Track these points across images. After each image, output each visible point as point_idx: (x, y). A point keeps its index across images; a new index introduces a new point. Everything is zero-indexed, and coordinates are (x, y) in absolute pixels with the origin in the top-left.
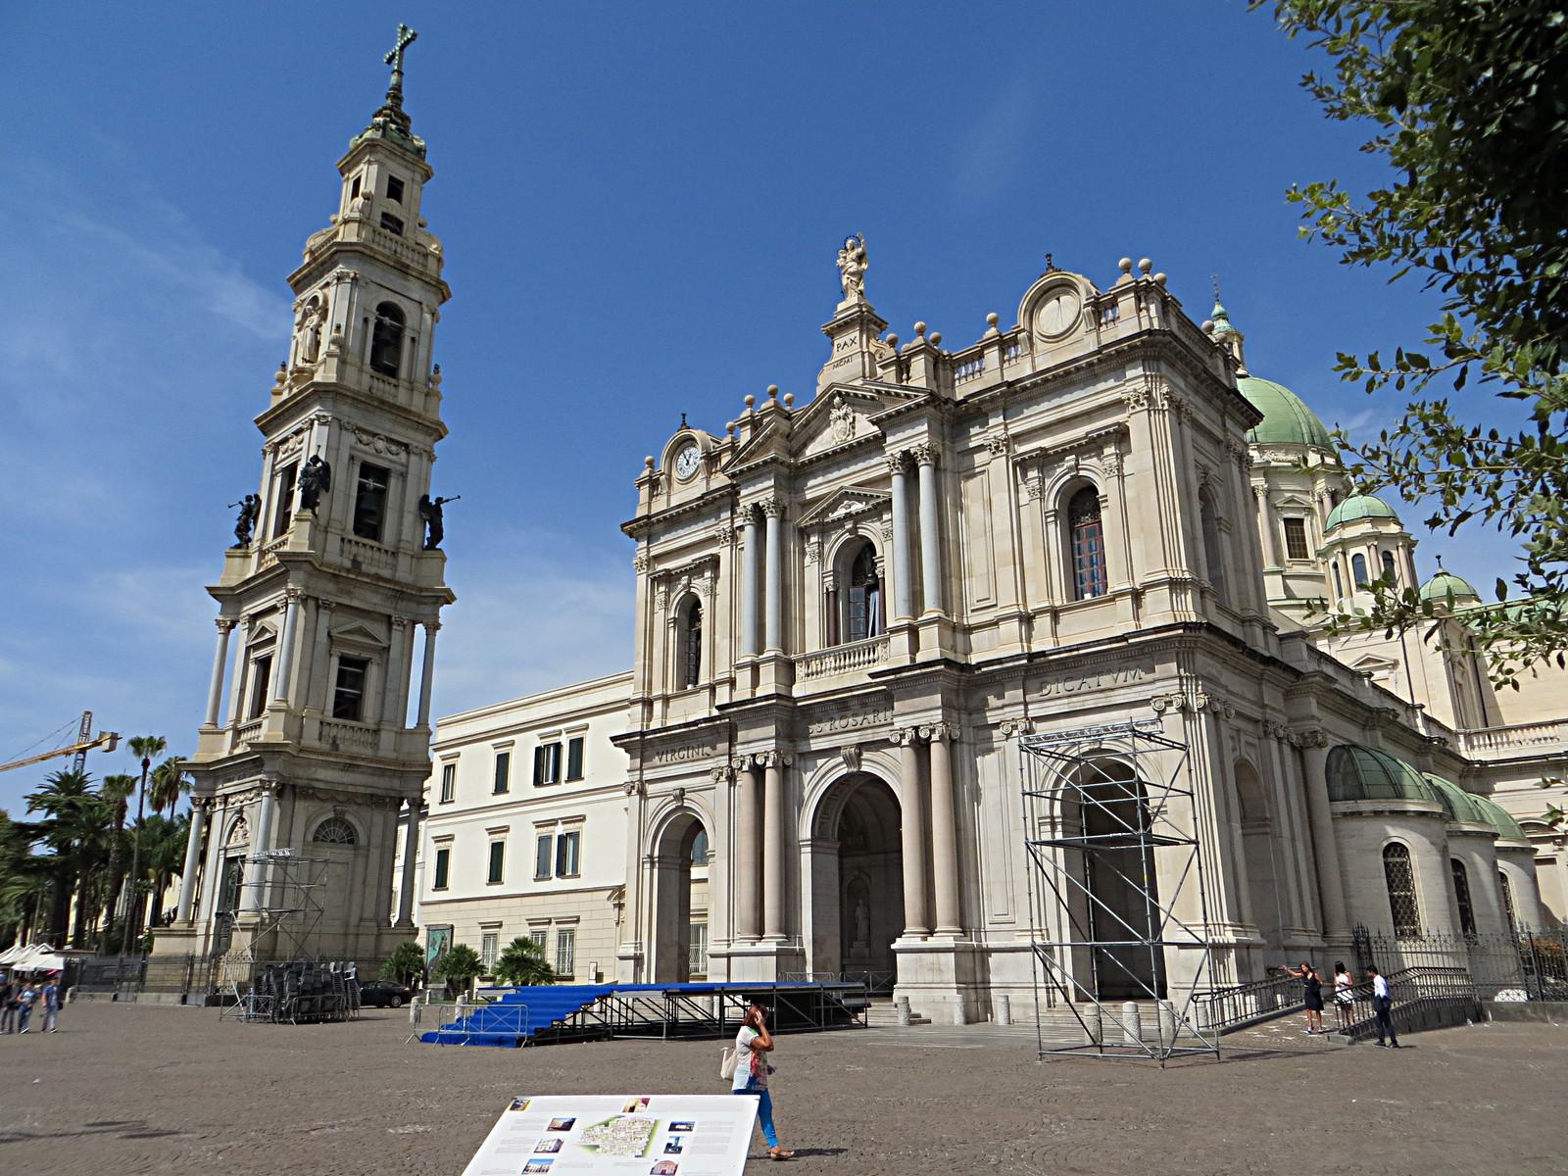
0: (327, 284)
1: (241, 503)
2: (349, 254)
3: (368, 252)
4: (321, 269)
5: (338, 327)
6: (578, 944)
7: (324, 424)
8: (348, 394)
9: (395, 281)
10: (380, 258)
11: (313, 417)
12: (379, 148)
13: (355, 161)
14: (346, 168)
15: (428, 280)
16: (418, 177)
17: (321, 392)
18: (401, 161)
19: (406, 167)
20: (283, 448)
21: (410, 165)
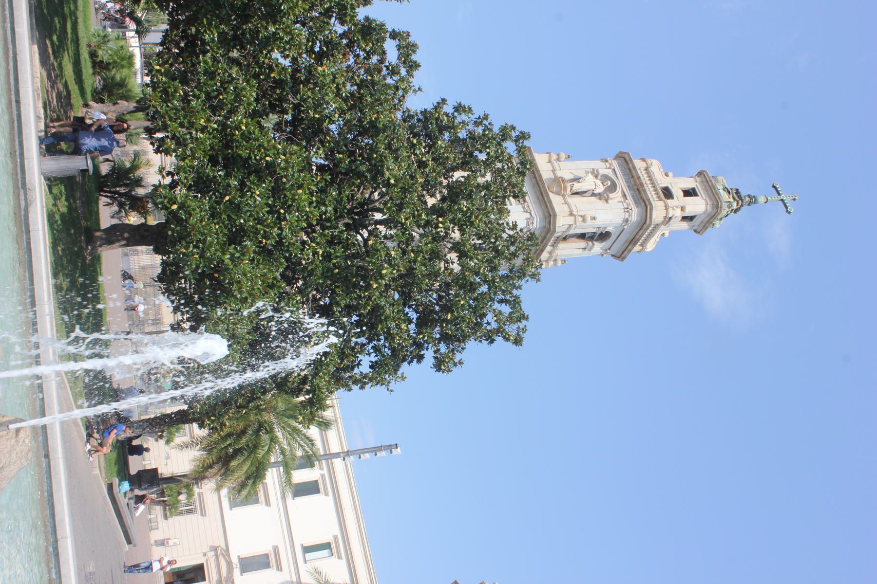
0: (624, 196)
2: (644, 214)
3: (645, 226)
4: (635, 187)
5: (594, 218)
6: (188, 517)
7: (528, 224)
8: (549, 235)
9: (624, 237)
10: (641, 232)
11: (533, 213)
12: (715, 210)
13: (708, 188)
14: (704, 180)
15: (626, 252)
16: (695, 228)
17: (549, 216)
18: (706, 220)
19: (702, 222)
21: (703, 224)
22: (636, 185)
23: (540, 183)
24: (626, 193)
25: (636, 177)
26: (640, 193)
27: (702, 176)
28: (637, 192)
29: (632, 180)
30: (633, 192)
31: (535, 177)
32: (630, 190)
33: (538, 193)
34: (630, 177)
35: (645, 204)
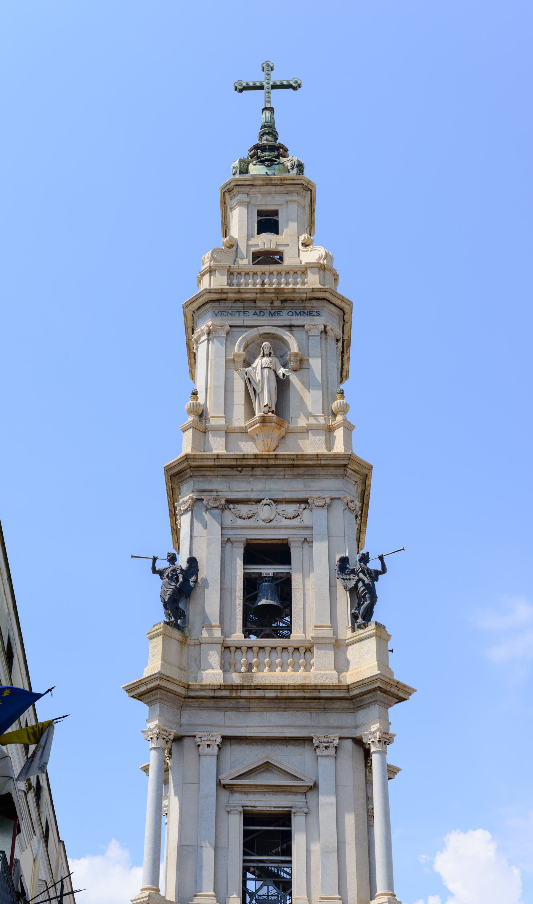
1: (155, 559)
4: (277, 304)
14: (247, 189)
20: (244, 510)
22: (272, 302)
23: (272, 462)
24: (288, 323)
25: (258, 295)
26: (292, 300)
27: (236, 190)
28: (289, 304)
29: (259, 304)
30: (285, 312)
31: (253, 467)
32: (279, 314)
33: (288, 472)
34: (253, 305)
35: (318, 299)
